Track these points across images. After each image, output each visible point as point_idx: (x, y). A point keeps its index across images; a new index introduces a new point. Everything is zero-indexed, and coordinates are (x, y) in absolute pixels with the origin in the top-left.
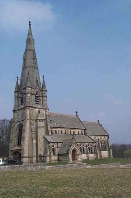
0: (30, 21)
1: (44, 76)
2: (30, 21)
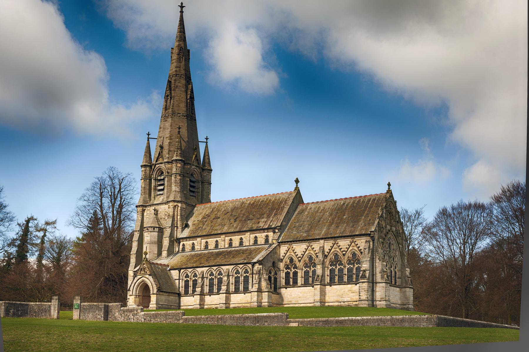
0: (182, 4)
1: (207, 139)
2: (182, 4)
